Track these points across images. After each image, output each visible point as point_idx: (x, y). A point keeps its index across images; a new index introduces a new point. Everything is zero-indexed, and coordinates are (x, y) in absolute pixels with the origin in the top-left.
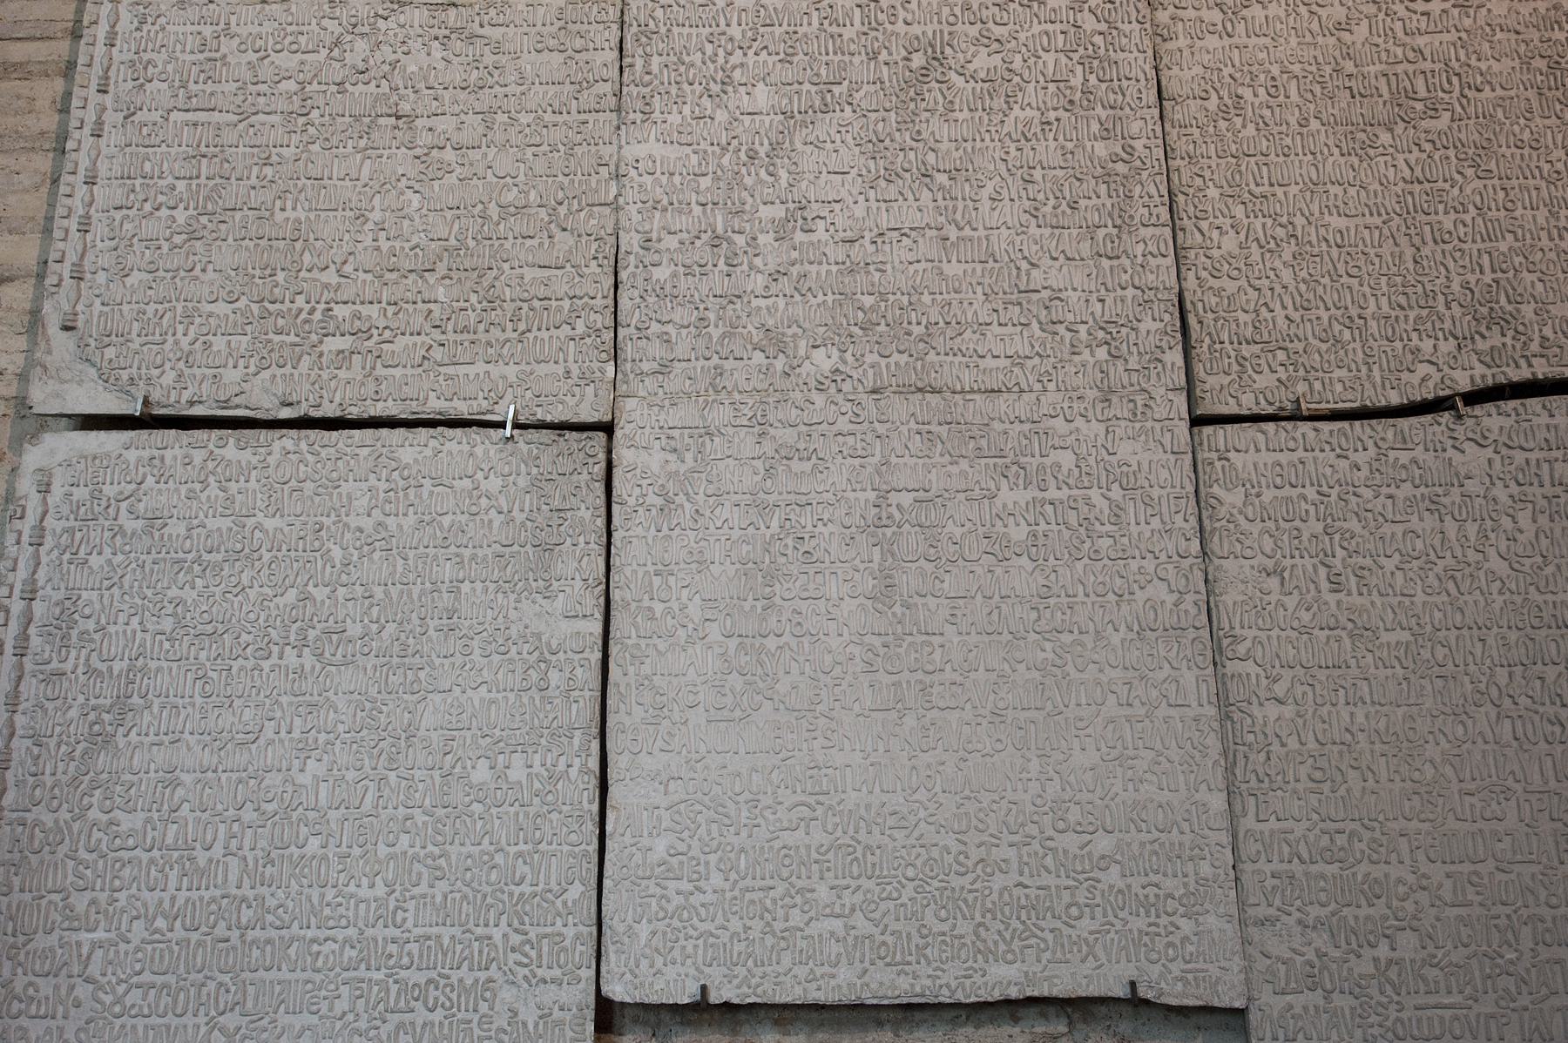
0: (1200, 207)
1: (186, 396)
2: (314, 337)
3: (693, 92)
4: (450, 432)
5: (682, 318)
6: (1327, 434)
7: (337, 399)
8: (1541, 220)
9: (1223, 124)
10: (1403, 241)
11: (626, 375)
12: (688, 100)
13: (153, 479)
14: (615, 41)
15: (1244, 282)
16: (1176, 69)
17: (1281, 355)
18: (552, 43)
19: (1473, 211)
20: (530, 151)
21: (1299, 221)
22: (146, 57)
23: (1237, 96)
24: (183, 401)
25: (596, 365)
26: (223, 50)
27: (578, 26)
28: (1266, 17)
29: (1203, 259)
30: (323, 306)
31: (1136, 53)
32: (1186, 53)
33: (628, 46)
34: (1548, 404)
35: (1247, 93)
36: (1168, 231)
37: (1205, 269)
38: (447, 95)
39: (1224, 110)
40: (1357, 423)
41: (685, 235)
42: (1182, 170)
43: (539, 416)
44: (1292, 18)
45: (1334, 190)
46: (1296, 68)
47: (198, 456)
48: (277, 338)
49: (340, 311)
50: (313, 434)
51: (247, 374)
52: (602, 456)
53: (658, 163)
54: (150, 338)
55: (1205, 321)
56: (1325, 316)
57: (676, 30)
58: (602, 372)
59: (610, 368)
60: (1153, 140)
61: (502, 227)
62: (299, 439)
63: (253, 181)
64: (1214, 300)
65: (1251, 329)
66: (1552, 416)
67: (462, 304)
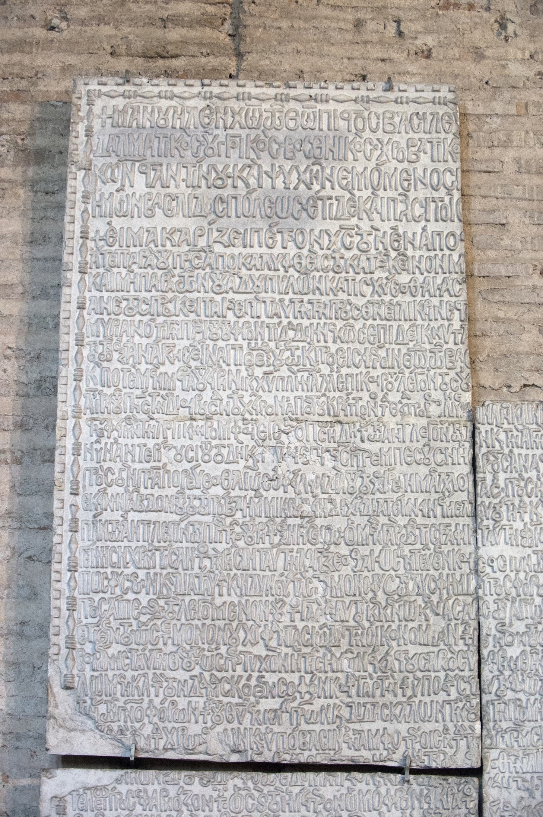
1: (162, 743)
2: (252, 699)
3: (531, 502)
4: (358, 775)
5: (530, 688)
7: (274, 749)
11: (489, 732)
12: (528, 510)
13: (141, 807)
14: (468, 458)
18: (418, 457)
20: (407, 549)
22: (106, 465)
24: (161, 747)
25: (467, 724)
26: (164, 460)
27: (438, 444)
30: (256, 674)
33: (480, 463)
38: (338, 499)
41: (530, 621)
43: (426, 763)
47: (173, 791)
48: (225, 700)
49: (271, 678)
50: (260, 776)
51: (207, 728)
52: (475, 795)
53: (508, 563)
54: (131, 698)
57: (516, 451)
58: (472, 728)
59: (478, 726)
61: (389, 611)
62: (247, 780)
63: (196, 570)
67: (362, 673)
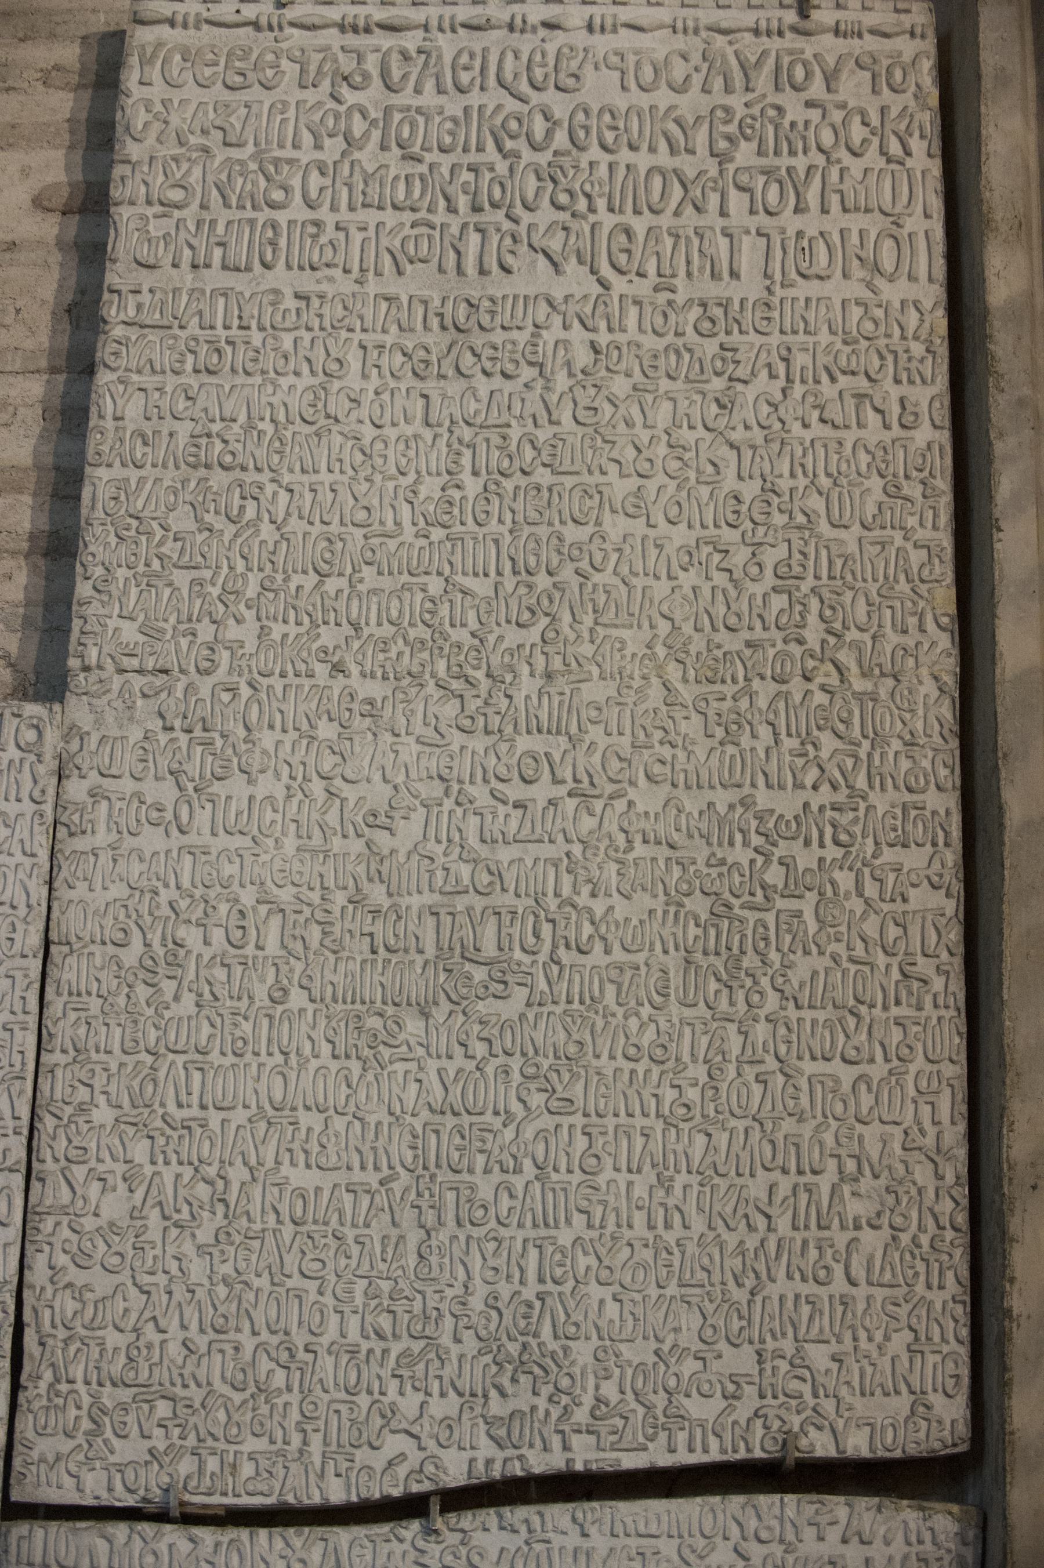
0: (76, 1143)
6: (210, 1550)
8: (640, 1191)
9: (142, 992)
10: (407, 1217)
15: (125, 1277)
16: (82, 887)
17: (163, 1409)
19: (529, 1168)
21: (238, 1174)
23: (175, 943)
28: (251, 798)
29: (66, 1233)
31: (19, 857)
32: (105, 858)
34: (579, 1515)
35: (192, 936)
36: (18, 1180)
37: (65, 1251)
39: (148, 969)
40: (263, 1533)
42: (59, 1073)
44: (295, 801)
45: (305, 1119)
46: (285, 895)
55: (50, 1342)
56: (249, 1344)
60: (21, 1017)
64: (71, 1306)
65: (122, 1360)
66: (585, 1535)
